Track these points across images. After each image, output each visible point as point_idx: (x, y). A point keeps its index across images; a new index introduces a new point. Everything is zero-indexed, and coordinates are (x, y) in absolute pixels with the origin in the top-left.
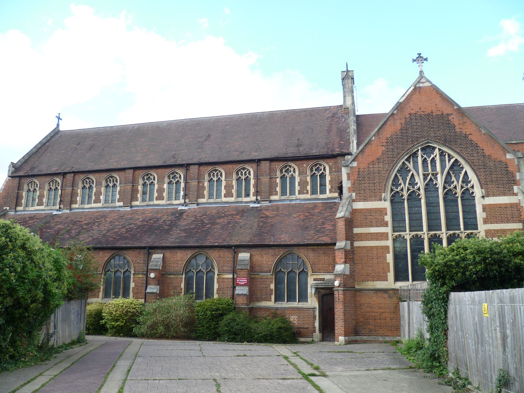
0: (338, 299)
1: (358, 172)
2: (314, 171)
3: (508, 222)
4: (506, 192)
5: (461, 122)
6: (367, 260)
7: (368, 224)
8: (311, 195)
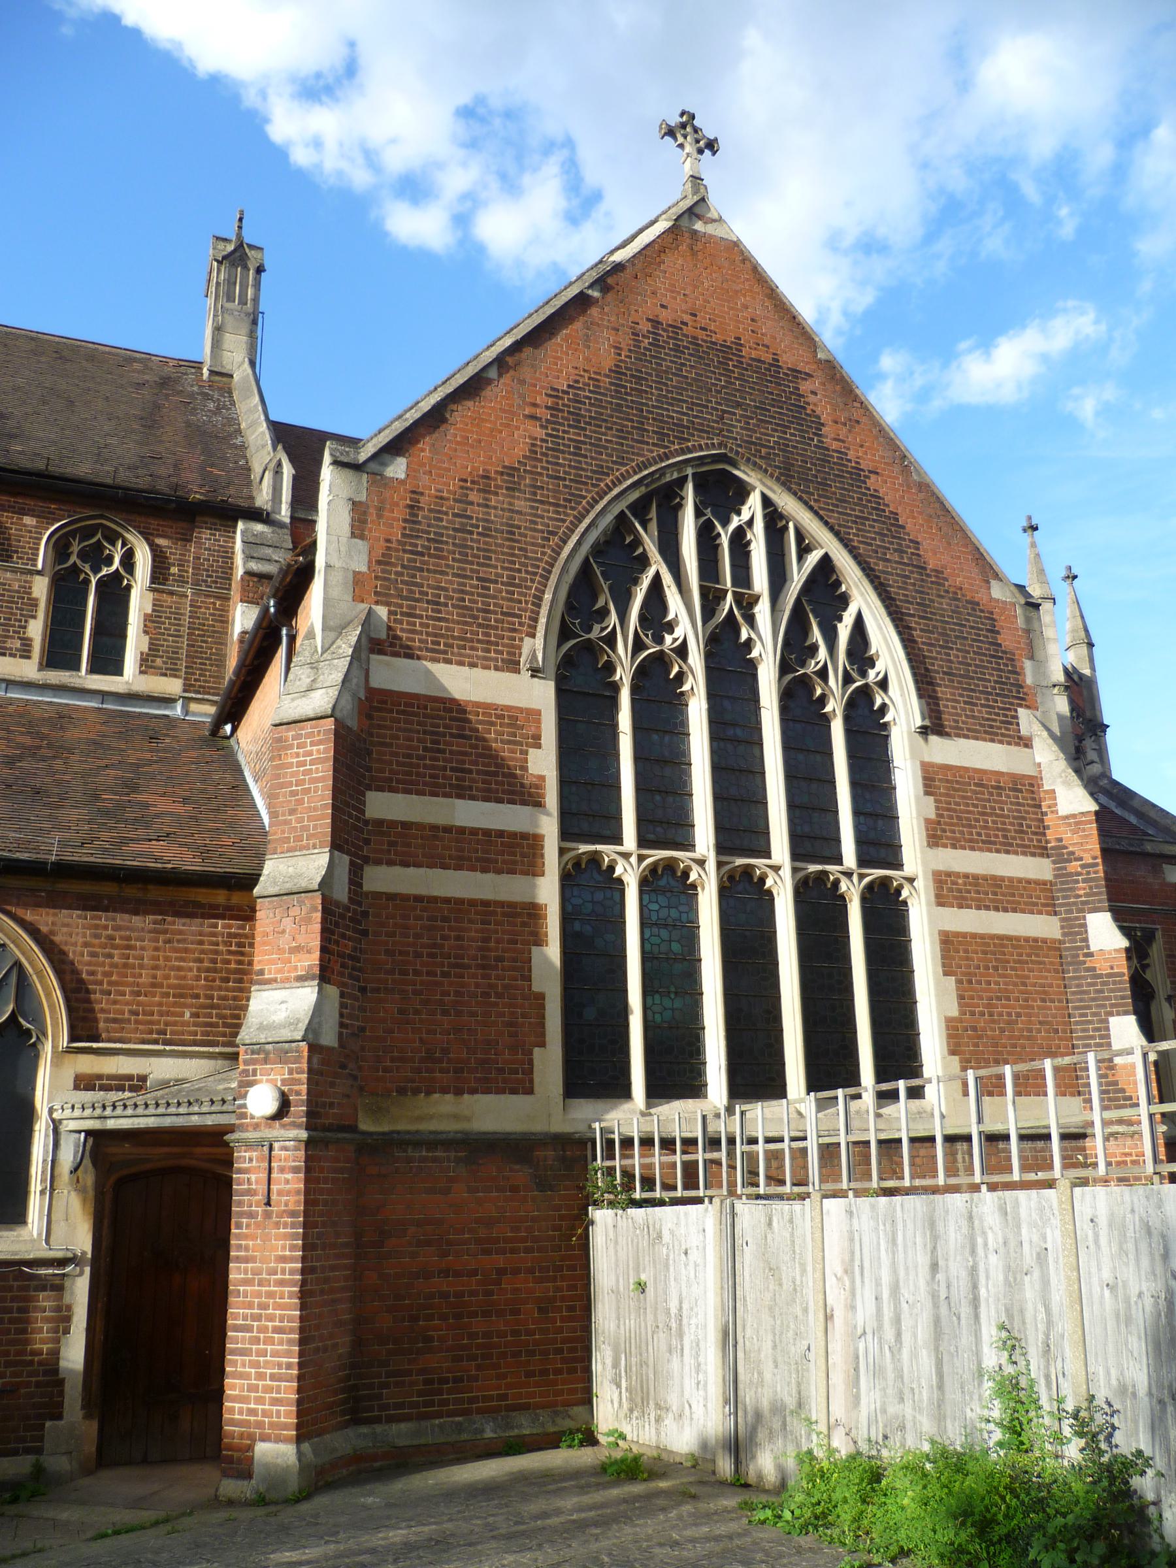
0: (260, 1197)
1: (411, 507)
2: (74, 558)
3: (1007, 847)
6: (428, 974)
7: (444, 777)
8: (41, 668)
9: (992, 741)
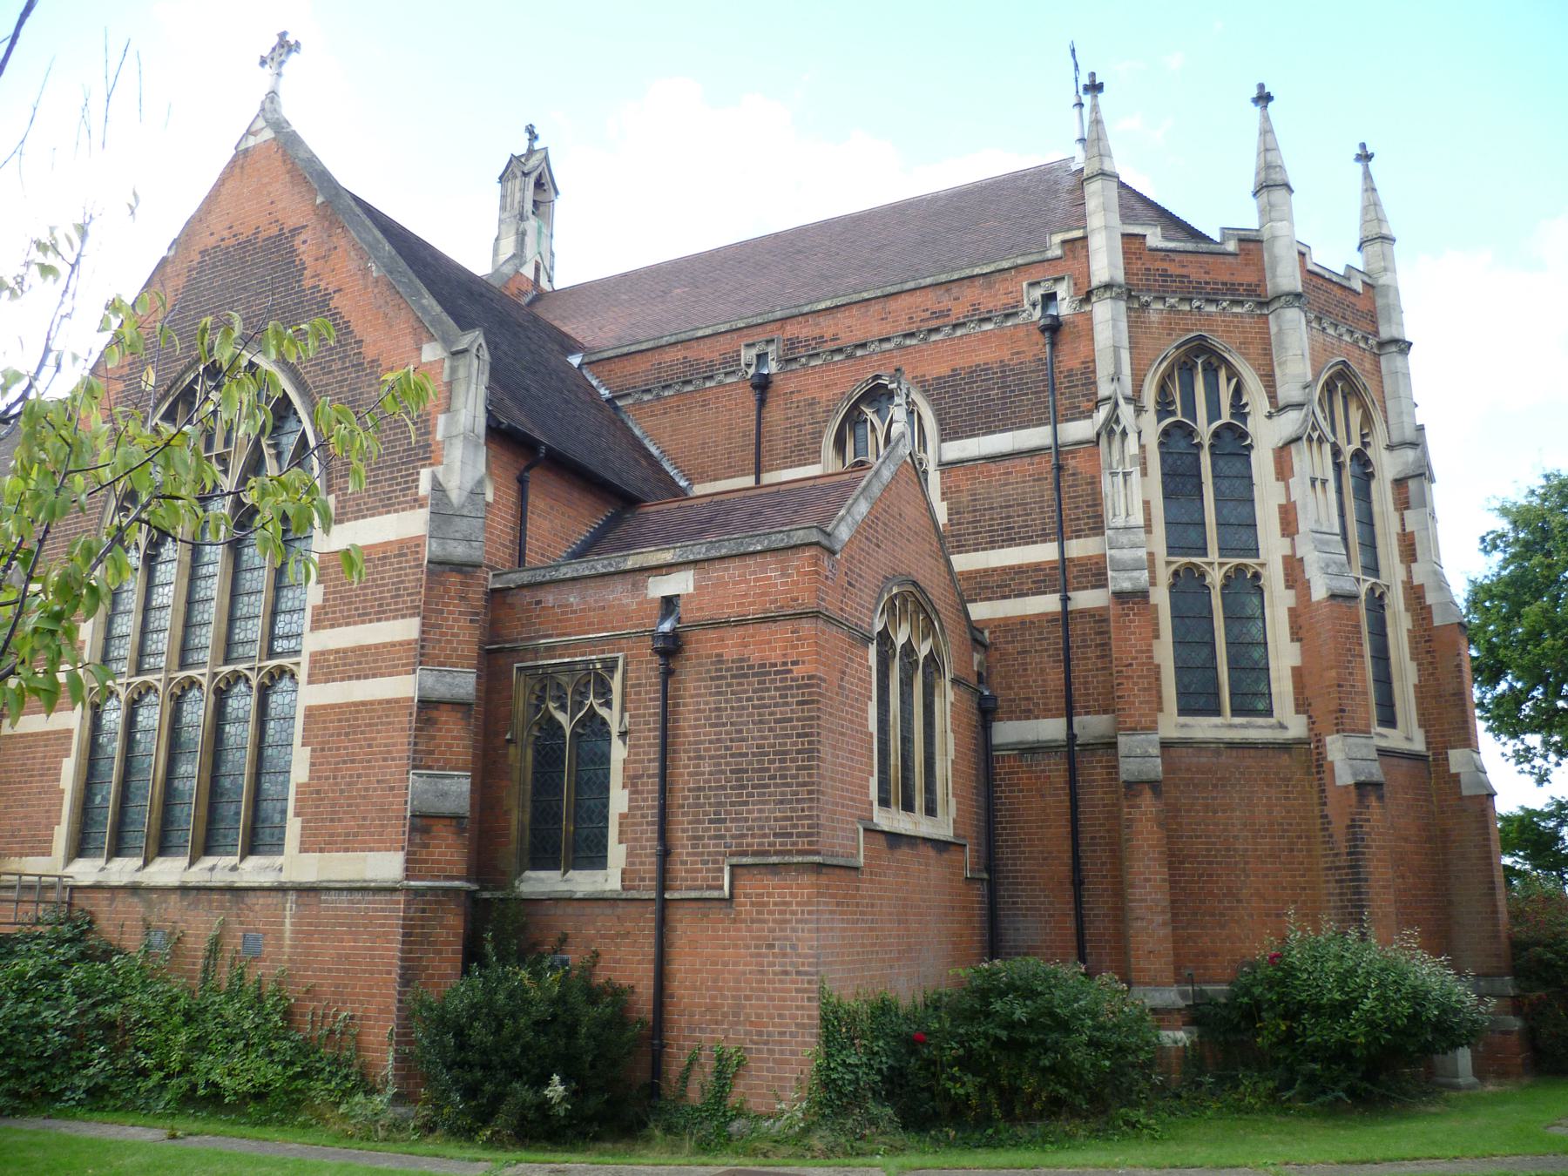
4: (396, 497)
5: (322, 252)
9: (388, 512)
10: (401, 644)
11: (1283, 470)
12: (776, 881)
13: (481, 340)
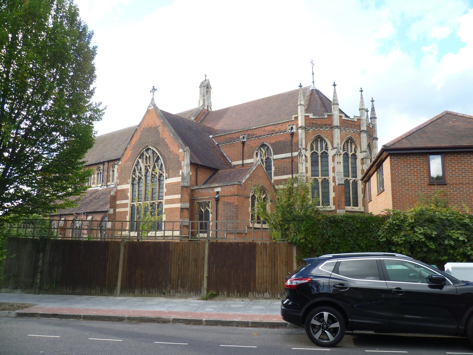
10: (178, 199)
11: (333, 161)
12: (232, 235)
13: (188, 148)
